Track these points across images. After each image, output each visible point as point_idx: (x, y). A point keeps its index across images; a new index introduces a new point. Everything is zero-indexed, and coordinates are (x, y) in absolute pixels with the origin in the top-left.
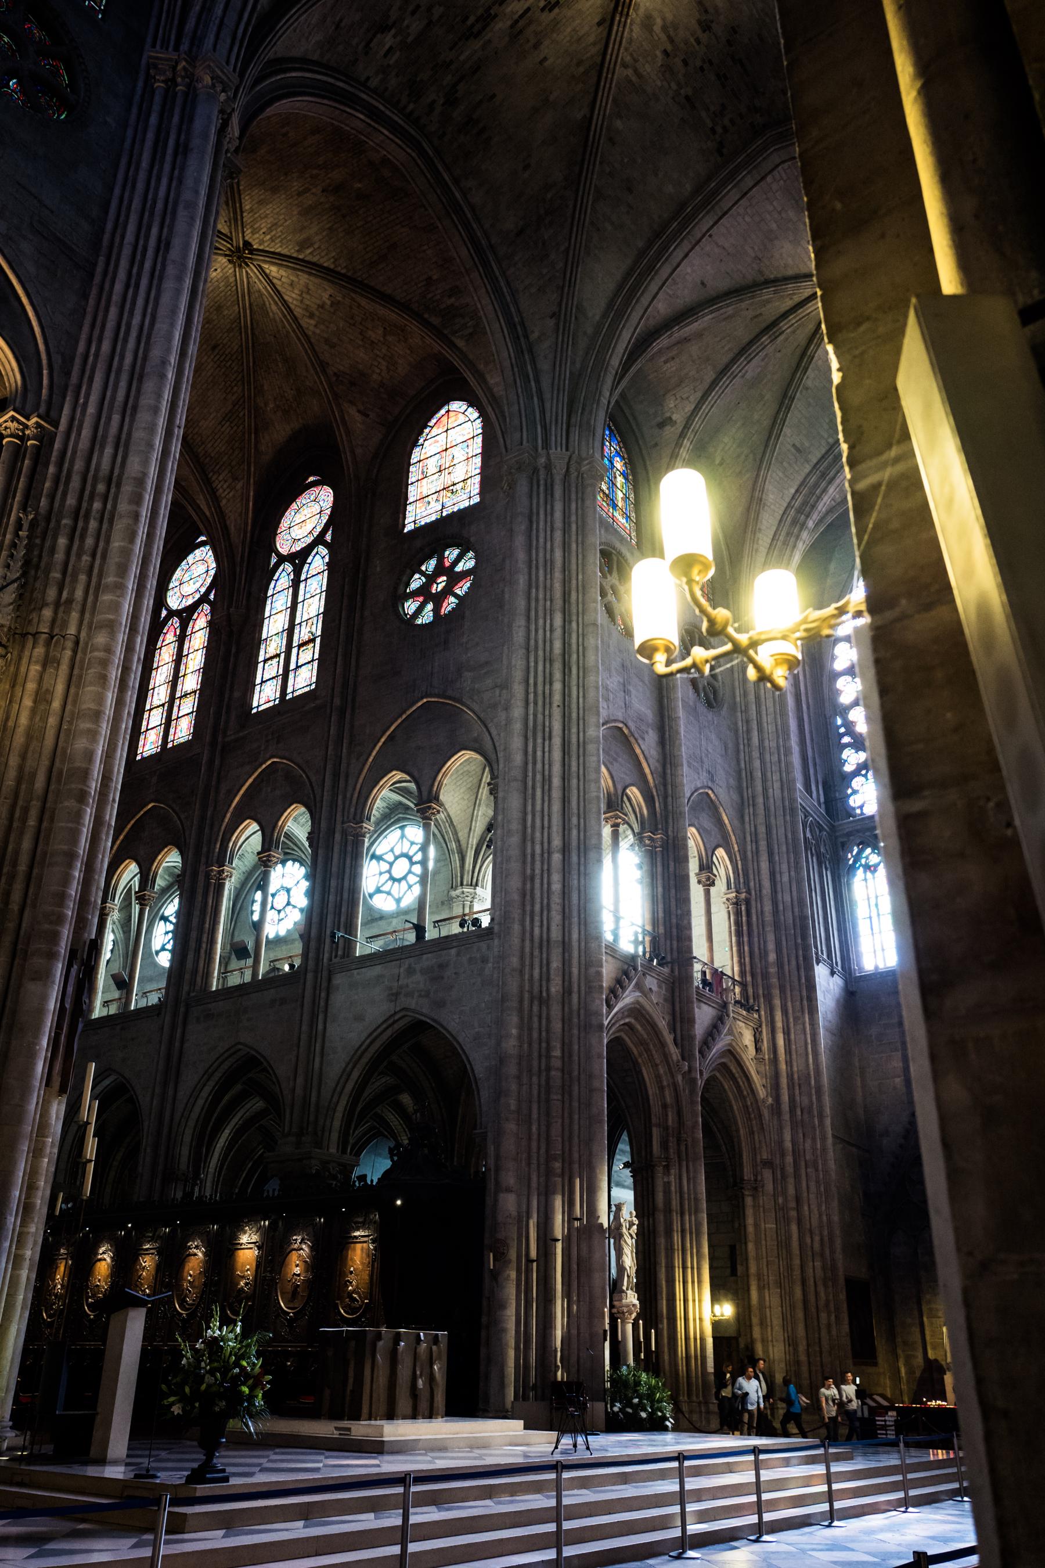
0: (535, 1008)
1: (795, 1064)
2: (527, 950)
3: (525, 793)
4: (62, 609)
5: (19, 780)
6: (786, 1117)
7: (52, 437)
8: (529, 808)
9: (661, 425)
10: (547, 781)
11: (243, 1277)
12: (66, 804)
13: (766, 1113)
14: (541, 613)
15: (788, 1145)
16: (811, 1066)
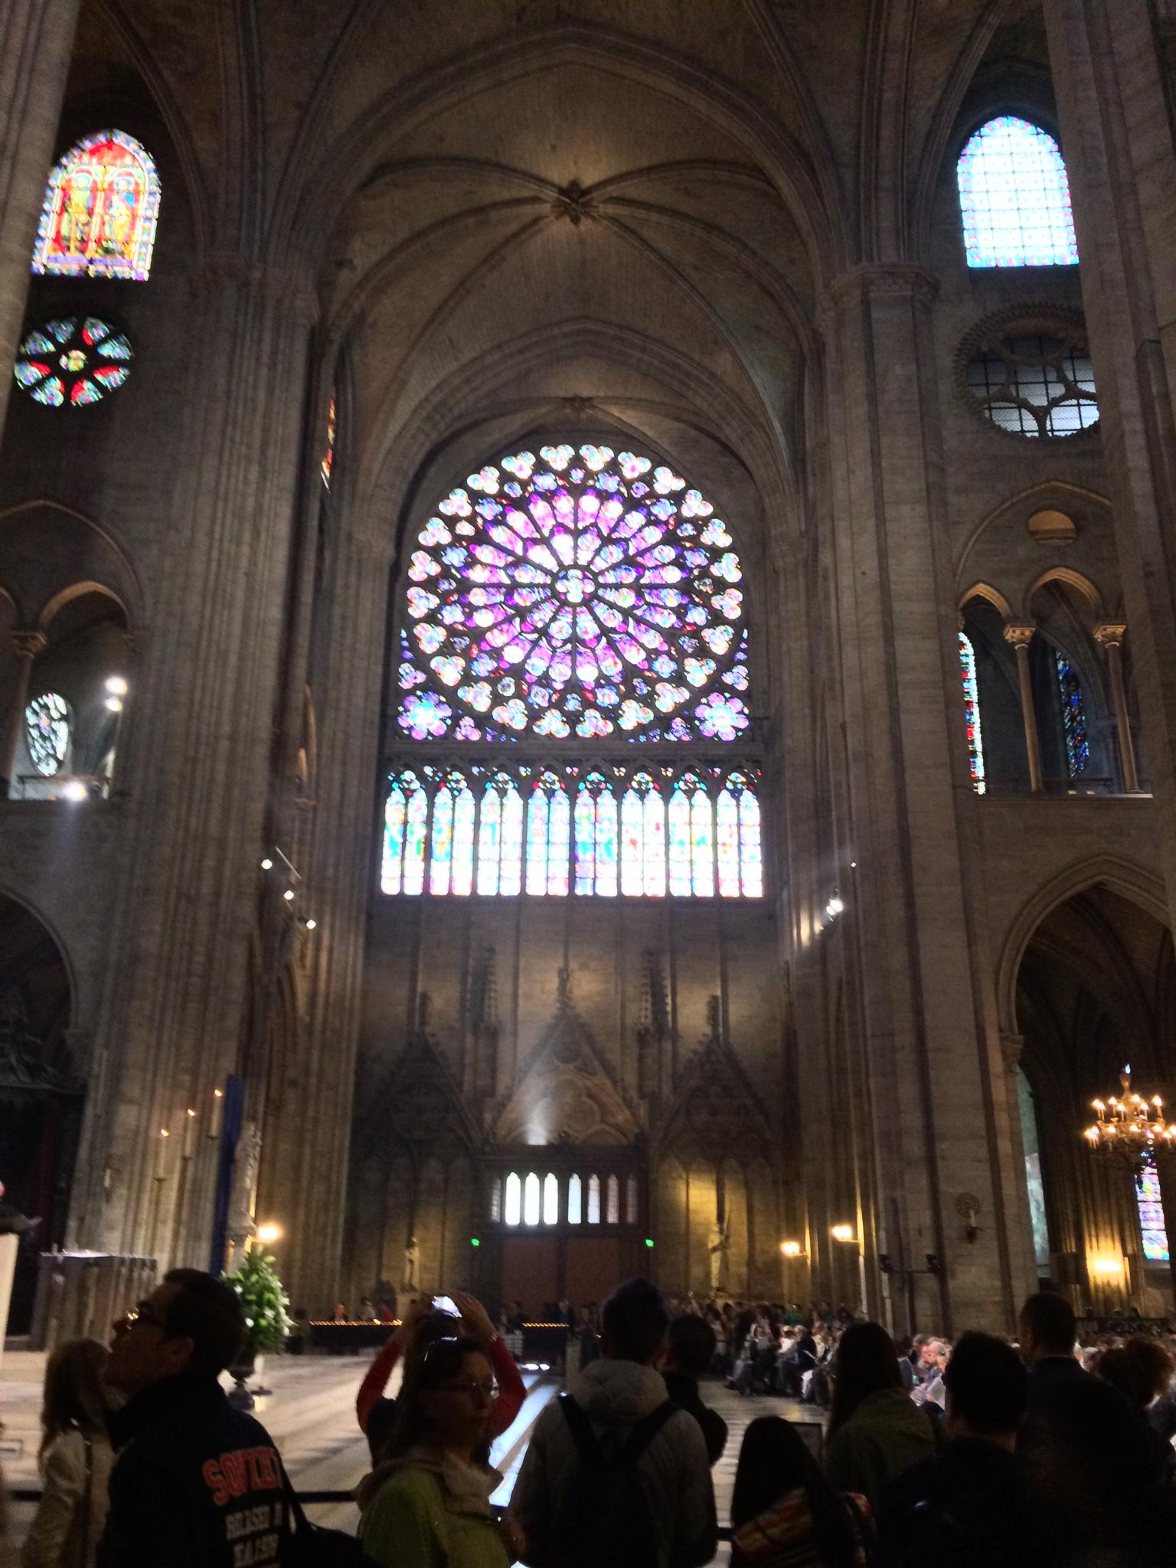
8: (199, 681)
9: (340, 264)
10: (223, 656)
13: (300, 1031)
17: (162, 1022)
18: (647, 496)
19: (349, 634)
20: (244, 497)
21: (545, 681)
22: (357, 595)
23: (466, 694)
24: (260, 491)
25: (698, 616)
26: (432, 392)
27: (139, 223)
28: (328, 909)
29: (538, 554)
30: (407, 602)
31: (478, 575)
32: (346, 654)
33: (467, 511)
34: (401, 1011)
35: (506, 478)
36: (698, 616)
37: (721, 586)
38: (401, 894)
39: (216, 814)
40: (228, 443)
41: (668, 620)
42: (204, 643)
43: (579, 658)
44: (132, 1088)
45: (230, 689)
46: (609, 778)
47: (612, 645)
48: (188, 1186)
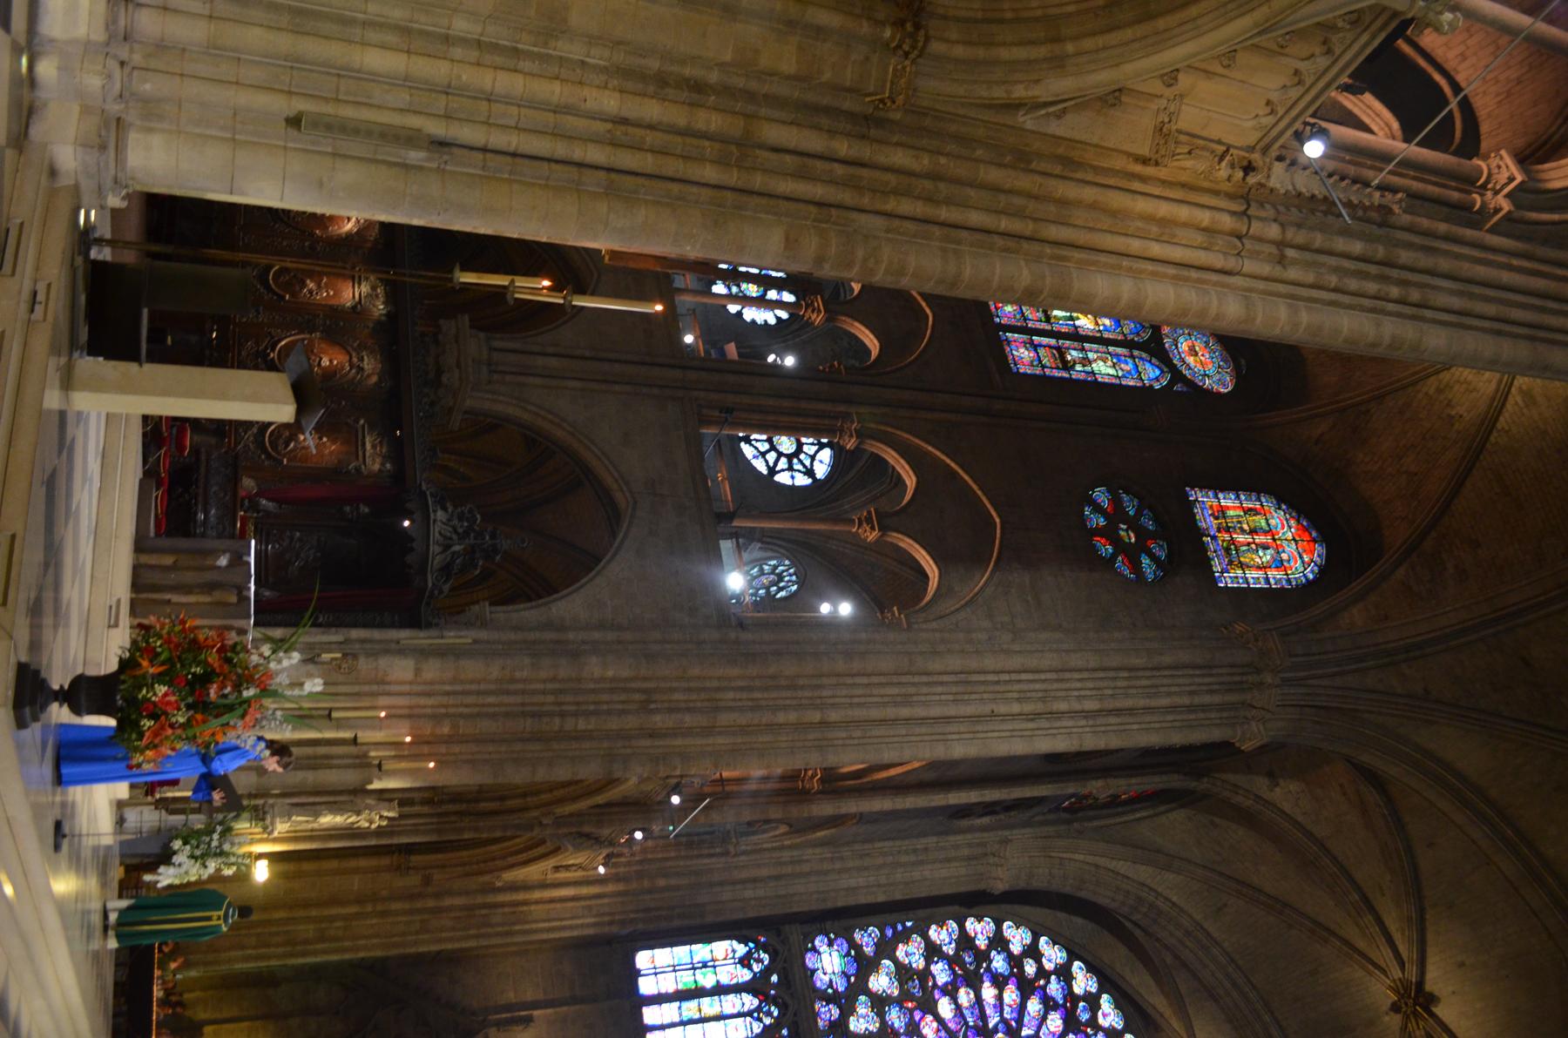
0: (637, 696)
1: (540, 907)
2: (708, 684)
3: (896, 674)
4: (1273, 250)
5: (1063, 203)
6: (480, 900)
7: (1476, 225)
8: (875, 680)
9: (1271, 775)
10: (906, 700)
11: (319, 286)
12: (1025, 272)
13: (487, 878)
15: (447, 902)
16: (534, 926)
17: (508, 693)
19: (912, 858)
20: (1065, 698)
22: (948, 860)
23: (863, 1007)
24: (1072, 714)
26: (1167, 899)
27: (1259, 574)
28: (621, 887)
30: (941, 924)
31: (988, 992)
32: (890, 859)
33: (1049, 966)
34: (511, 996)
35: (1093, 1001)
38: (637, 973)
39: (742, 719)
40: (1112, 674)
42: (916, 679)
44: (433, 670)
45: (875, 713)
48: (322, 750)
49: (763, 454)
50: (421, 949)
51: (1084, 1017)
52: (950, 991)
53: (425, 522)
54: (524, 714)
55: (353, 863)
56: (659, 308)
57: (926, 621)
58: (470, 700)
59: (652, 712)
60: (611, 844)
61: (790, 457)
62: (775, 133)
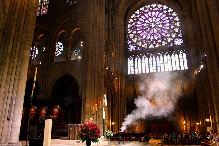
0: (93, 73)
5: (21, 6)
6: (119, 95)
14: (96, 5)
15: (119, 99)
17: (91, 91)
18: (162, 10)
21: (150, 40)
25: (172, 27)
29: (147, 21)
31: (138, 26)
32: (118, 38)
33: (135, 17)
34: (133, 91)
35: (140, 11)
36: (172, 27)
37: (176, 22)
38: (131, 74)
41: (168, 28)
43: (155, 36)
44: (88, 101)
46: (161, 53)
47: (159, 33)
49: (58, 52)
50: (125, 103)
51: (142, 12)
52: (137, 31)
53: (67, 102)
54: (94, 88)
55: (113, 112)
56: (36, 68)
57: (84, 30)
58: (92, 96)
59: (95, 71)
60: (113, 77)
61: (59, 49)
62: (10, 51)
